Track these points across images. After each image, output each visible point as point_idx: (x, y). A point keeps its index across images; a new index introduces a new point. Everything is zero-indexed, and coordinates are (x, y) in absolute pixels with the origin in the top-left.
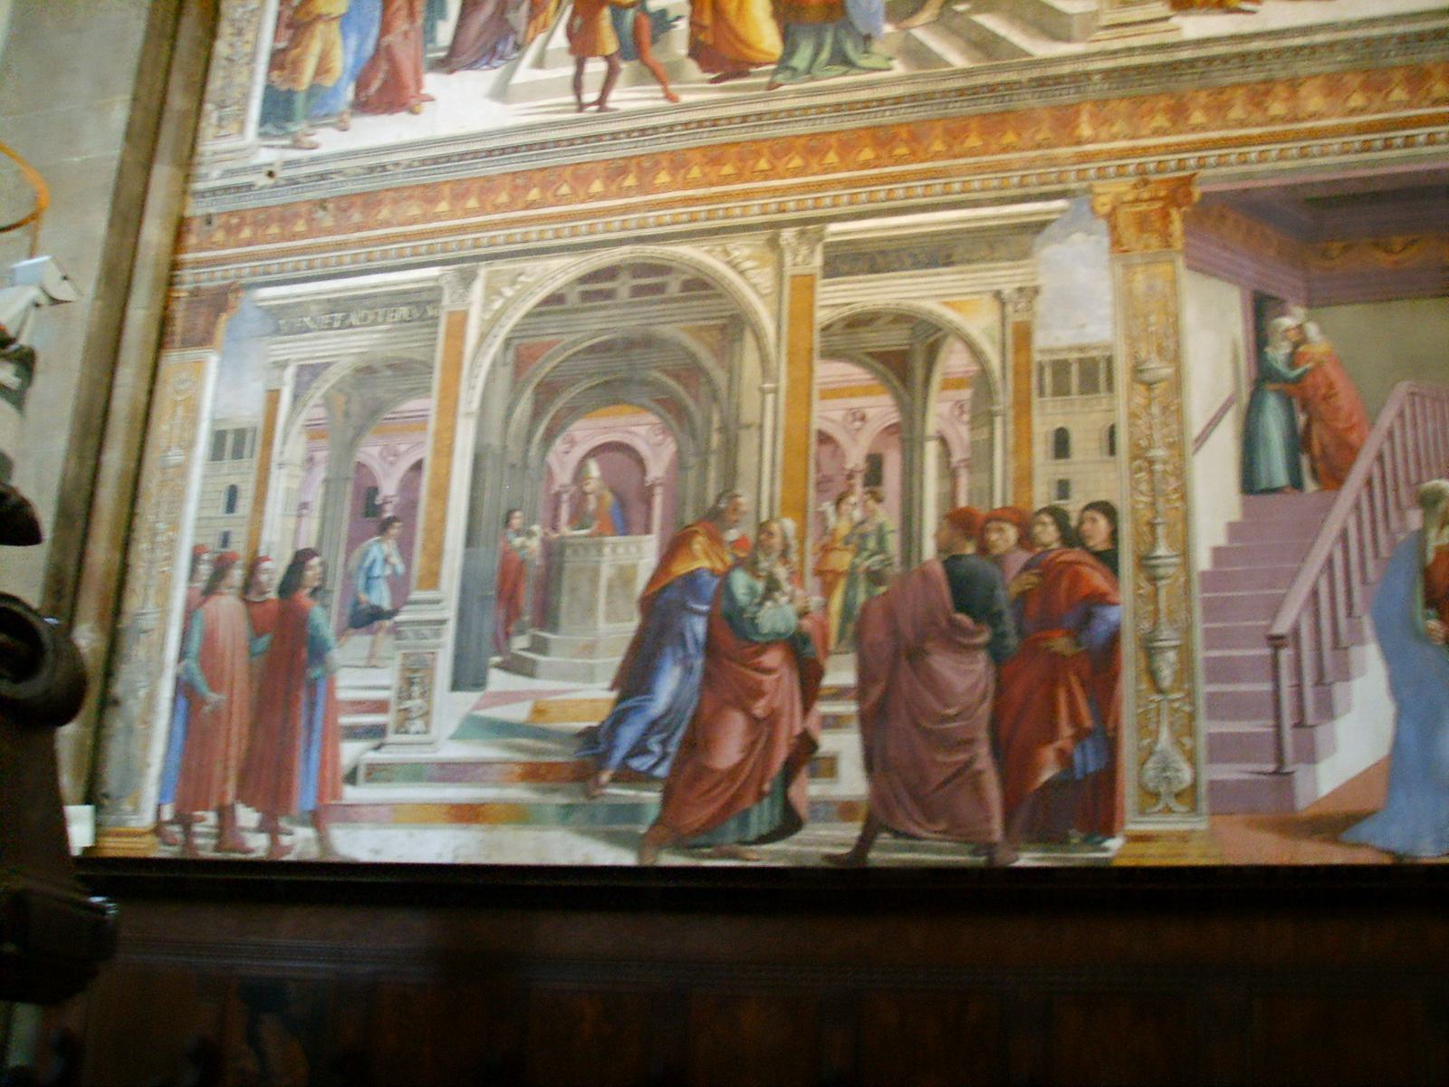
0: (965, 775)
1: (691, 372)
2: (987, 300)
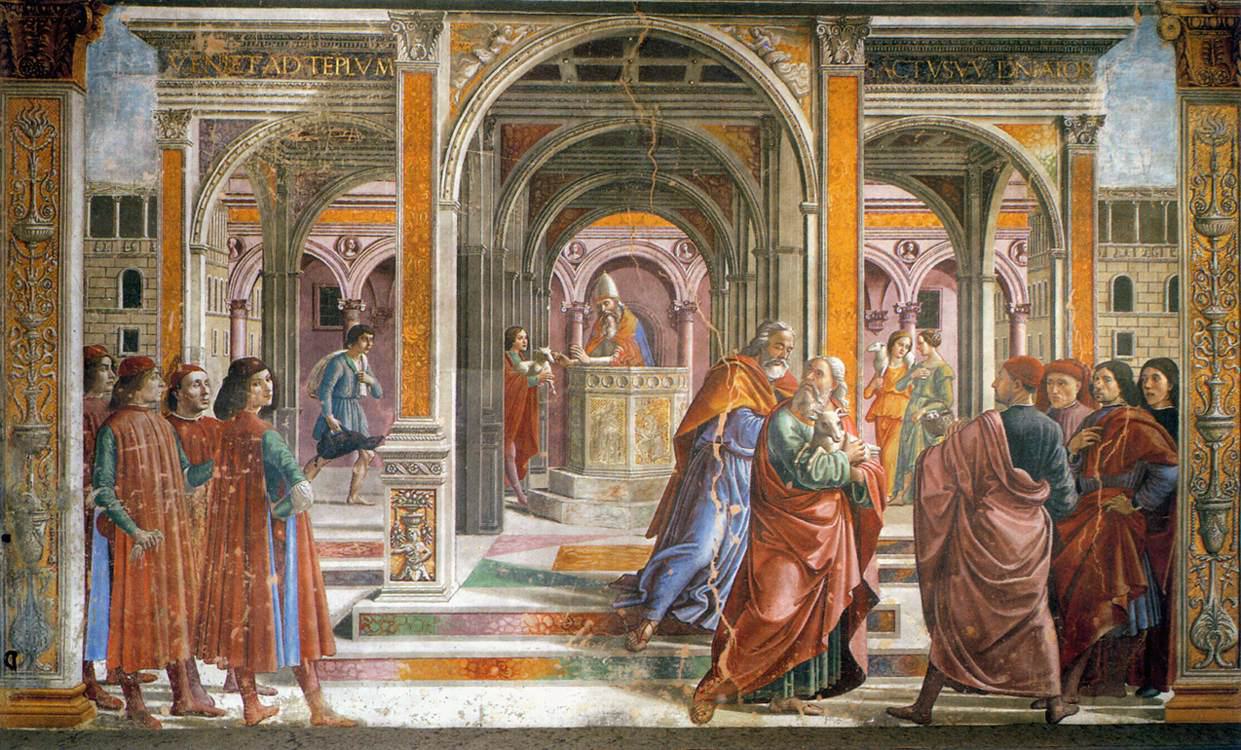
0: (1027, 631)
1: (721, 180)
2: (1049, 131)
